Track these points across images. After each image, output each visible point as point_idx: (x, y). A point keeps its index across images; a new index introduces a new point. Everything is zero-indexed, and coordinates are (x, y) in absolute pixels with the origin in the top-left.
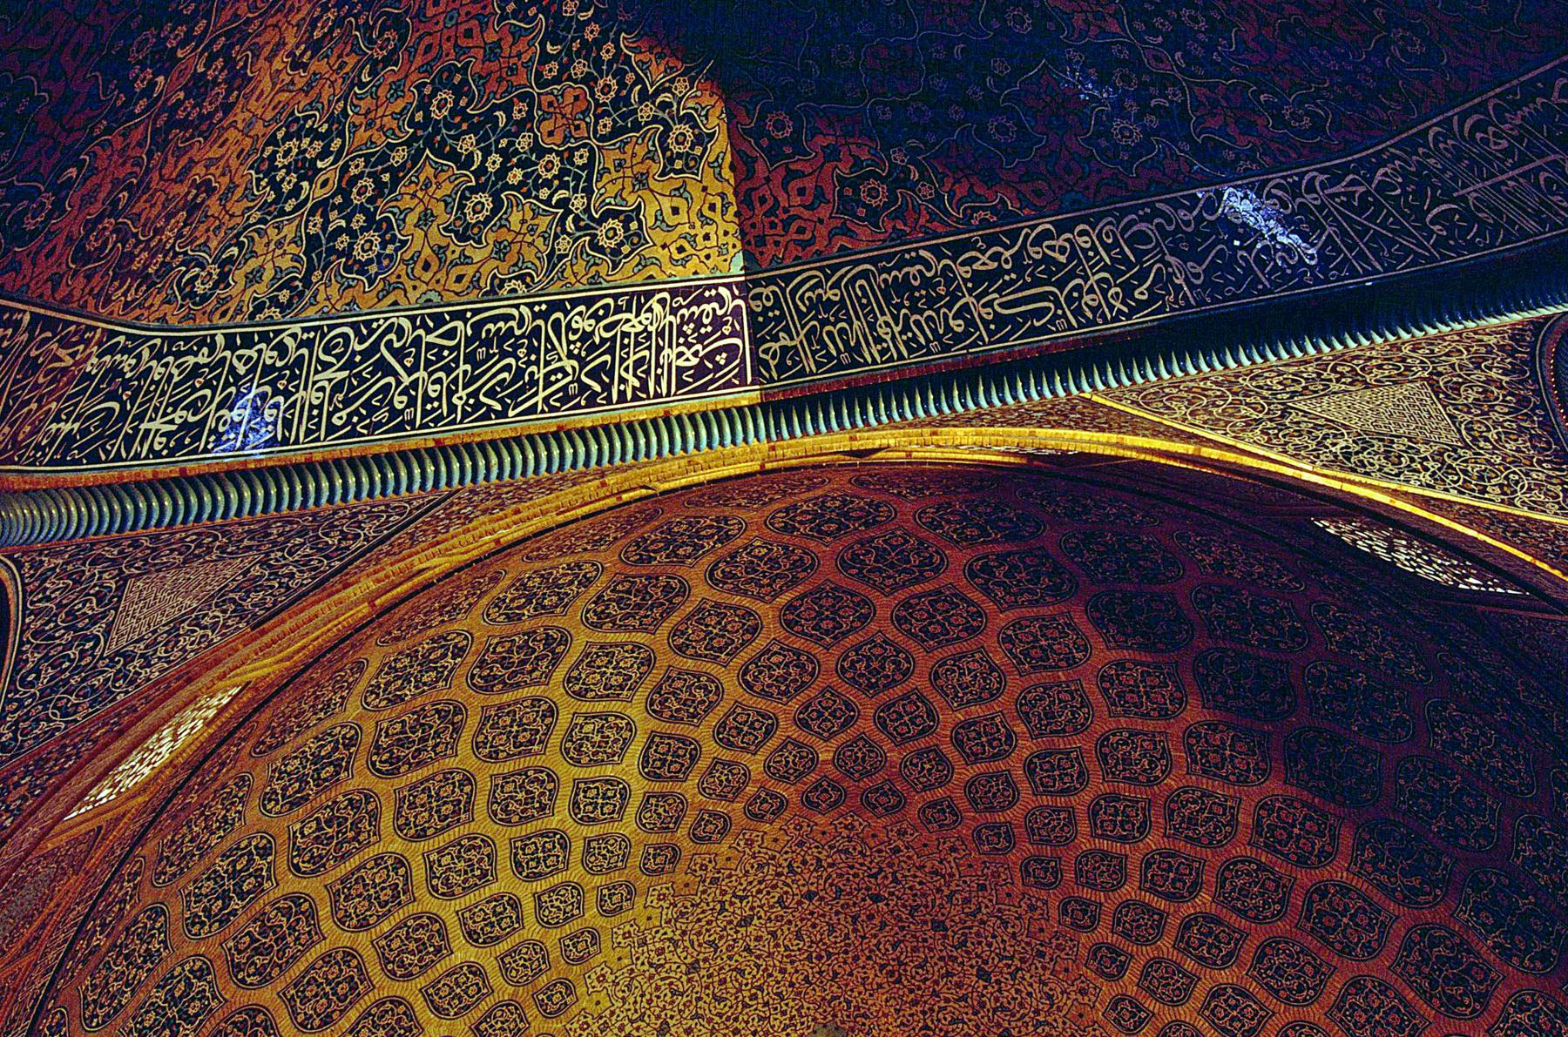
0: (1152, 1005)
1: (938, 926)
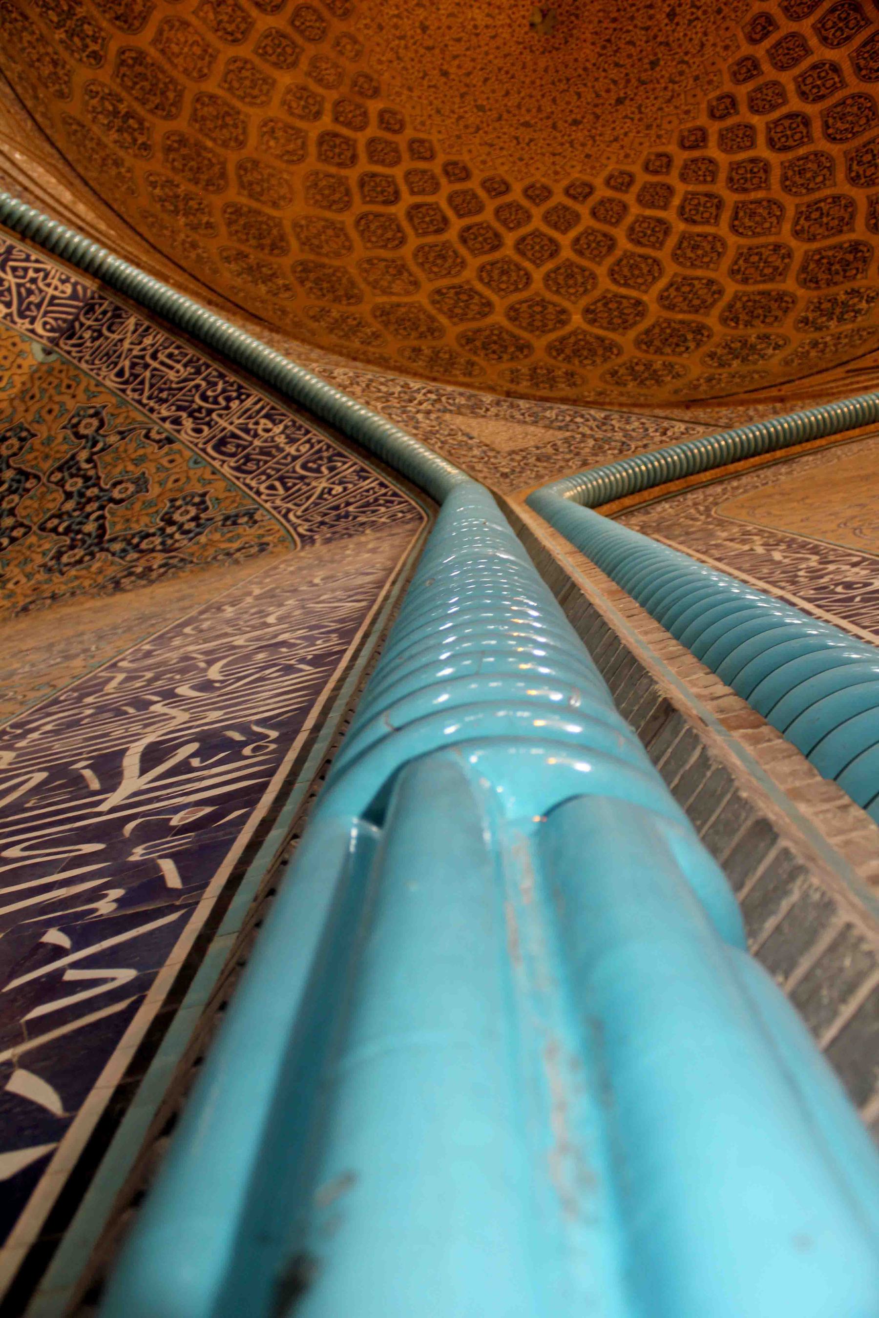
0: (766, 67)
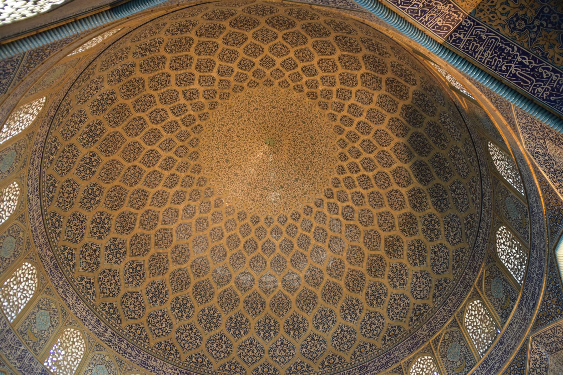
0: (342, 184)
1: (312, 137)
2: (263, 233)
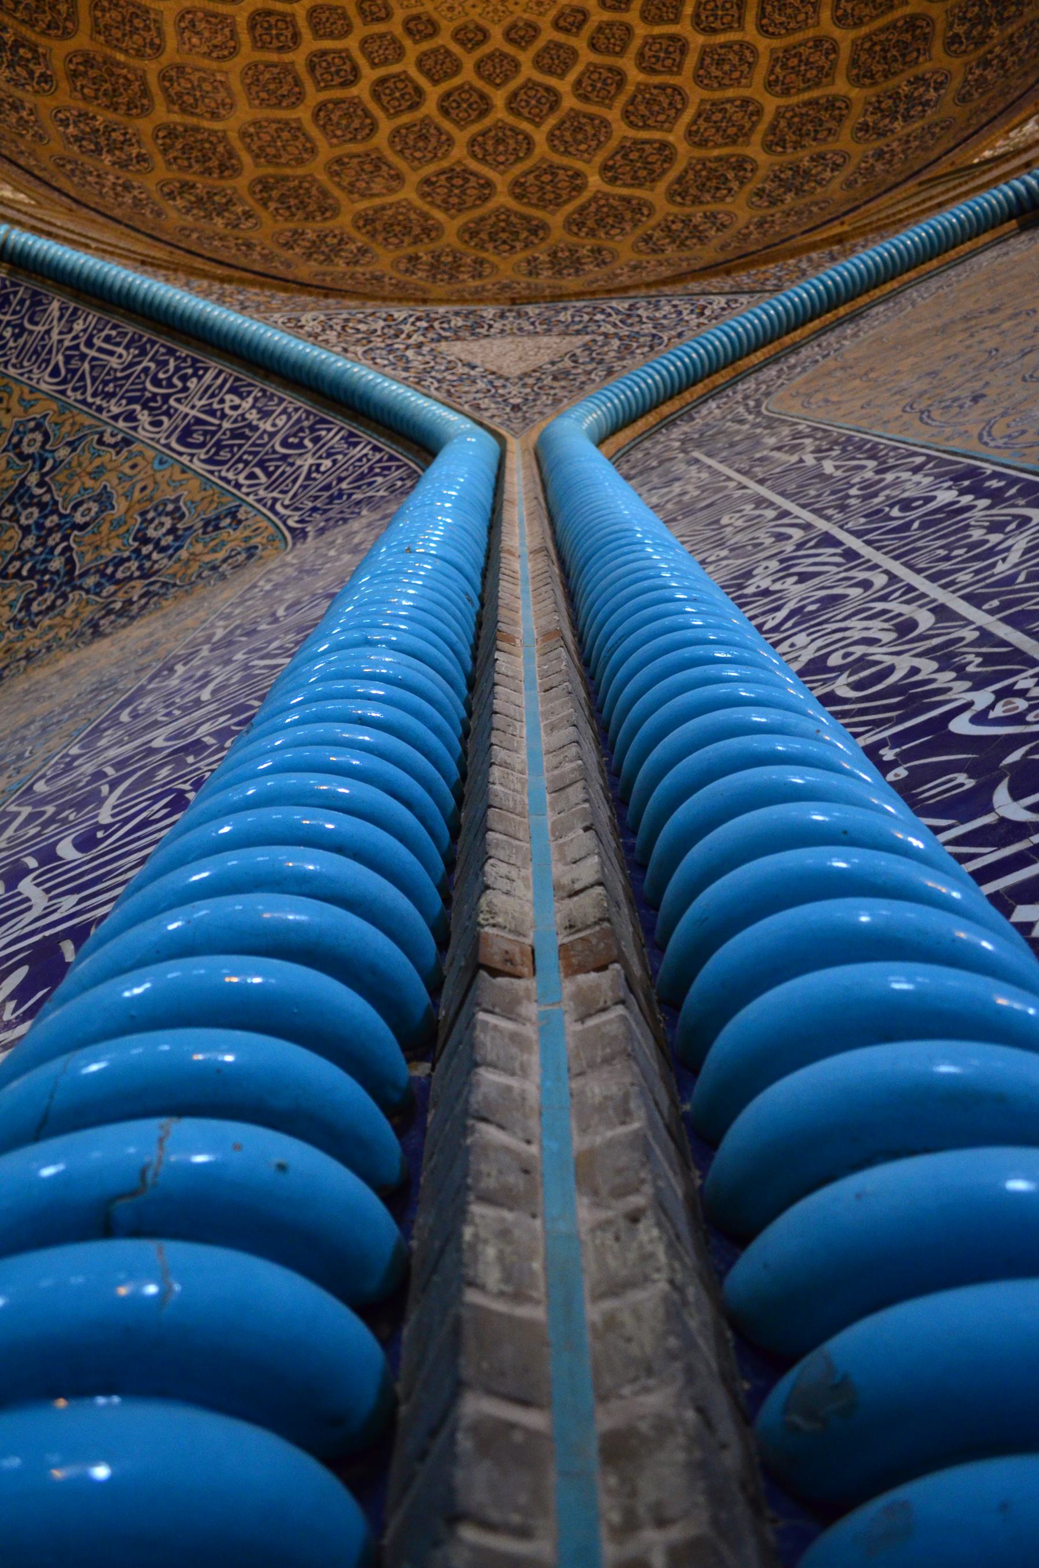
2: (506, 66)
